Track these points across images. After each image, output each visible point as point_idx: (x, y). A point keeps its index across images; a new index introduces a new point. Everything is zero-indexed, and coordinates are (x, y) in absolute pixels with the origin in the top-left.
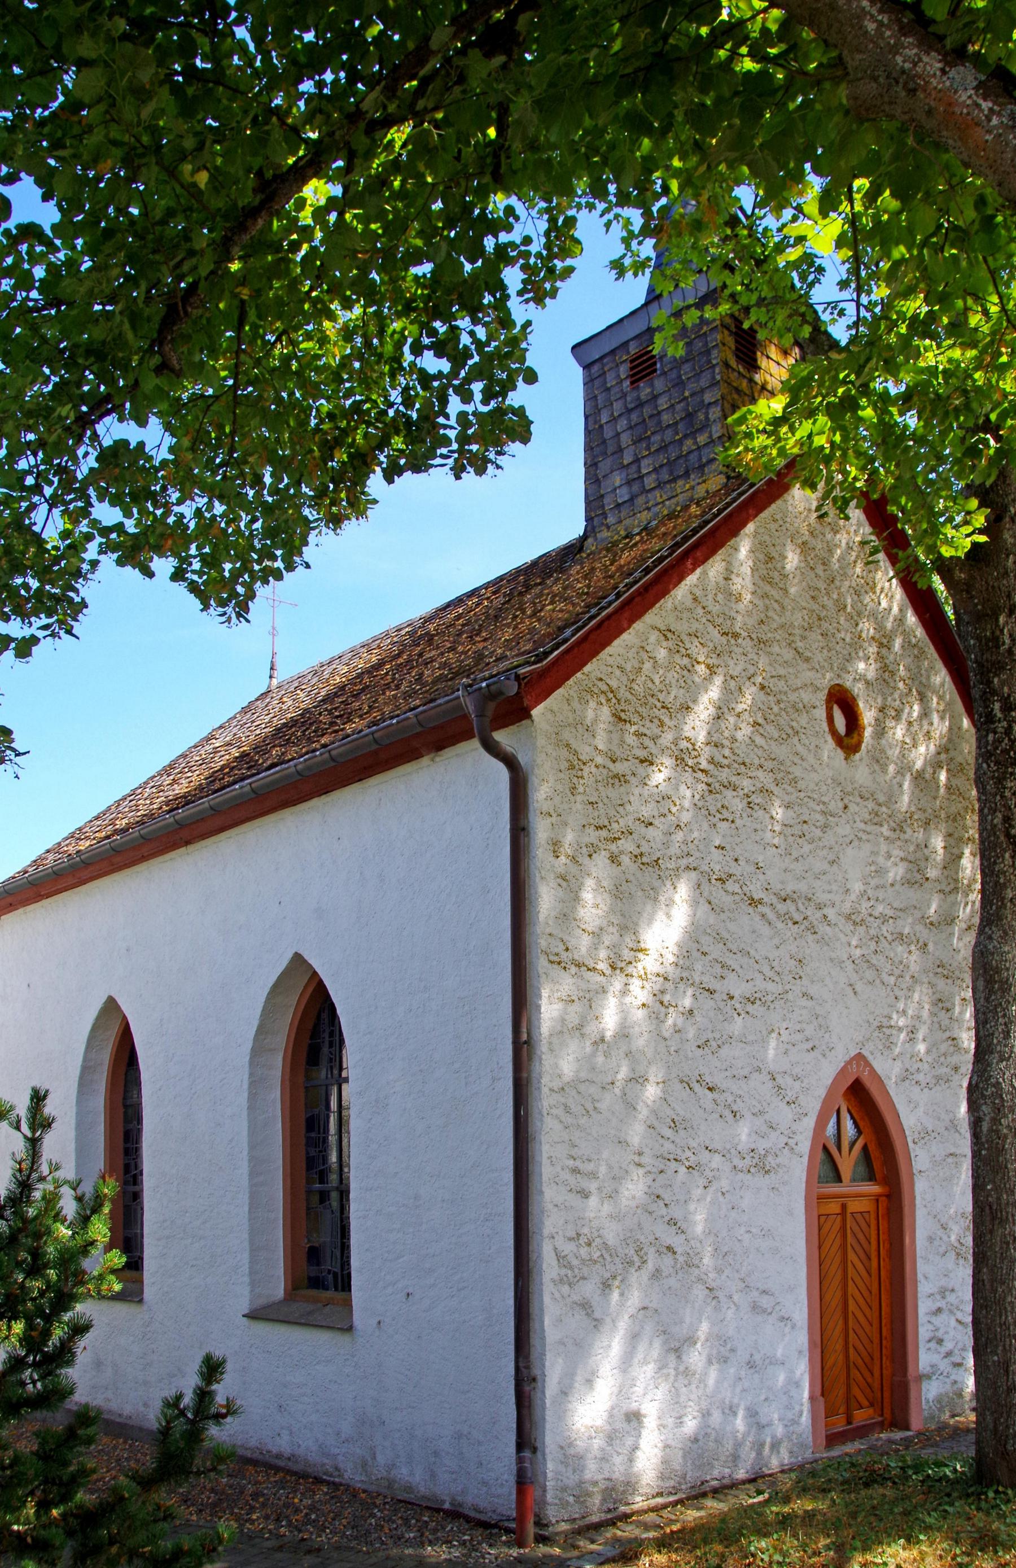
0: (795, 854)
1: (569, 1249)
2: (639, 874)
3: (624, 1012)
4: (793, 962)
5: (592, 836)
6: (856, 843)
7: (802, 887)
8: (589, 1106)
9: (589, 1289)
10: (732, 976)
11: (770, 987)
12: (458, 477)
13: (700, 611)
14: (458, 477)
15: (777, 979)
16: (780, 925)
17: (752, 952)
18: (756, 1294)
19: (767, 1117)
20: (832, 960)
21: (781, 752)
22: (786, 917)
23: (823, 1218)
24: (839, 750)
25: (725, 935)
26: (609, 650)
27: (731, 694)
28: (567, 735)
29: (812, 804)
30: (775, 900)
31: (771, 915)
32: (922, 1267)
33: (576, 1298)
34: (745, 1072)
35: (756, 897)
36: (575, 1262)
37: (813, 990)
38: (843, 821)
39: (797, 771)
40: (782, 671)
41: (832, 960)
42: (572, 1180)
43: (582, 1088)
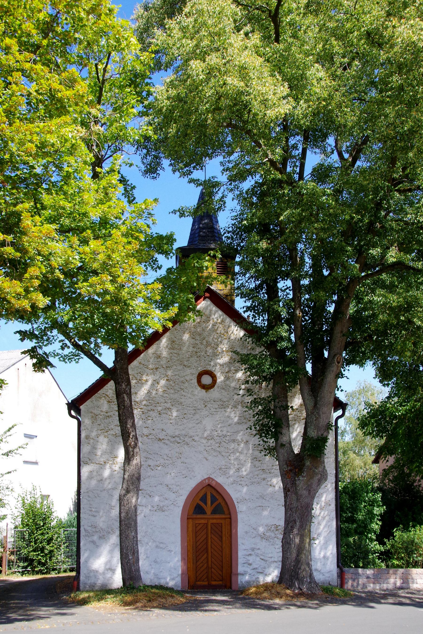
0: (180, 424)
1: (89, 529)
2: (115, 439)
3: (113, 471)
4: (177, 454)
5: (99, 432)
6: (211, 416)
7: (183, 432)
8: (96, 495)
9: (95, 538)
10: (150, 460)
11: (167, 461)
12: (174, 173)
13: (142, 366)
14: (174, 173)
15: (169, 459)
16: (171, 444)
17: (159, 453)
18: (158, 543)
19: (164, 497)
20: (196, 452)
21: (176, 396)
22: (173, 442)
23: (197, 525)
24: (203, 390)
25: (148, 450)
26: (107, 385)
27: (156, 382)
28: (91, 410)
29: (188, 408)
30: (170, 438)
31: (167, 442)
32: (240, 541)
33: (91, 540)
34: (155, 485)
35: (161, 438)
36: (90, 532)
37: (186, 461)
38: (204, 410)
39: (182, 400)
40: (177, 373)
41: (196, 452)
42: (90, 513)
43: (94, 491)
